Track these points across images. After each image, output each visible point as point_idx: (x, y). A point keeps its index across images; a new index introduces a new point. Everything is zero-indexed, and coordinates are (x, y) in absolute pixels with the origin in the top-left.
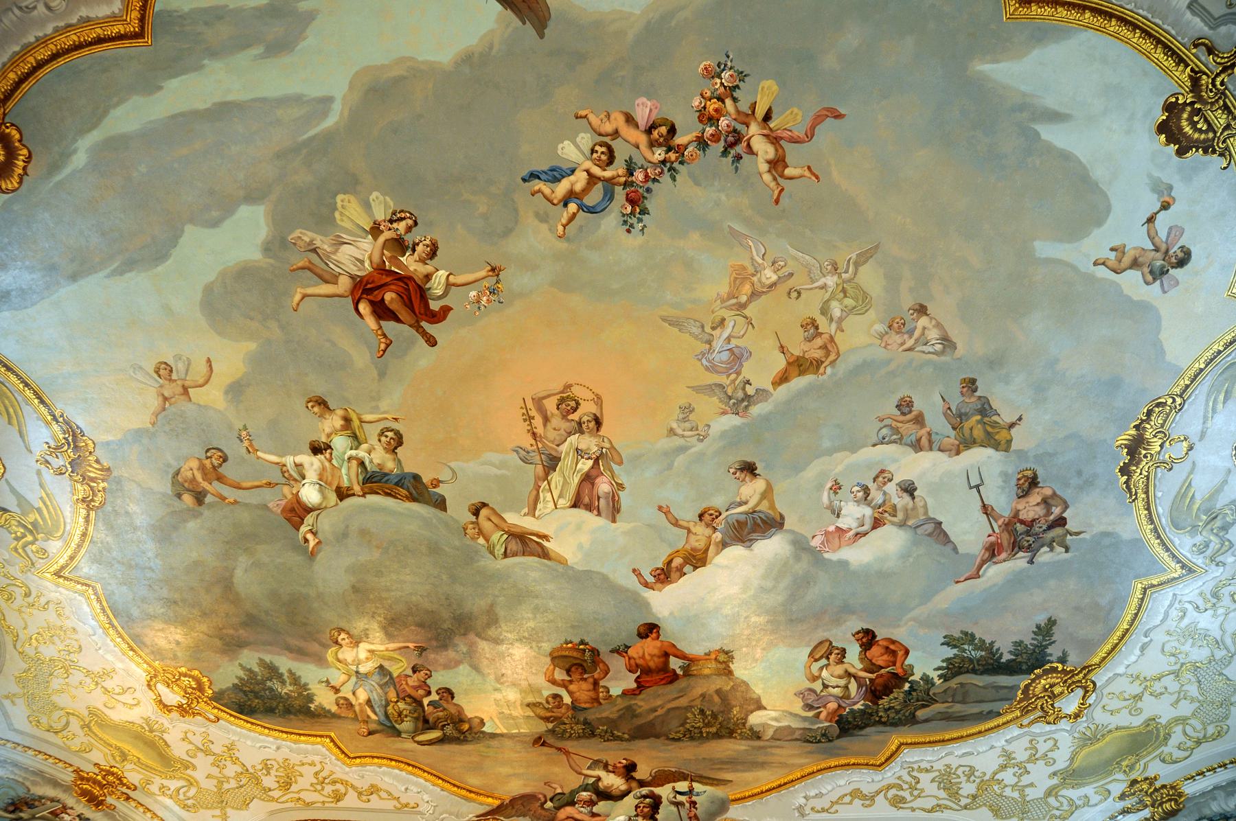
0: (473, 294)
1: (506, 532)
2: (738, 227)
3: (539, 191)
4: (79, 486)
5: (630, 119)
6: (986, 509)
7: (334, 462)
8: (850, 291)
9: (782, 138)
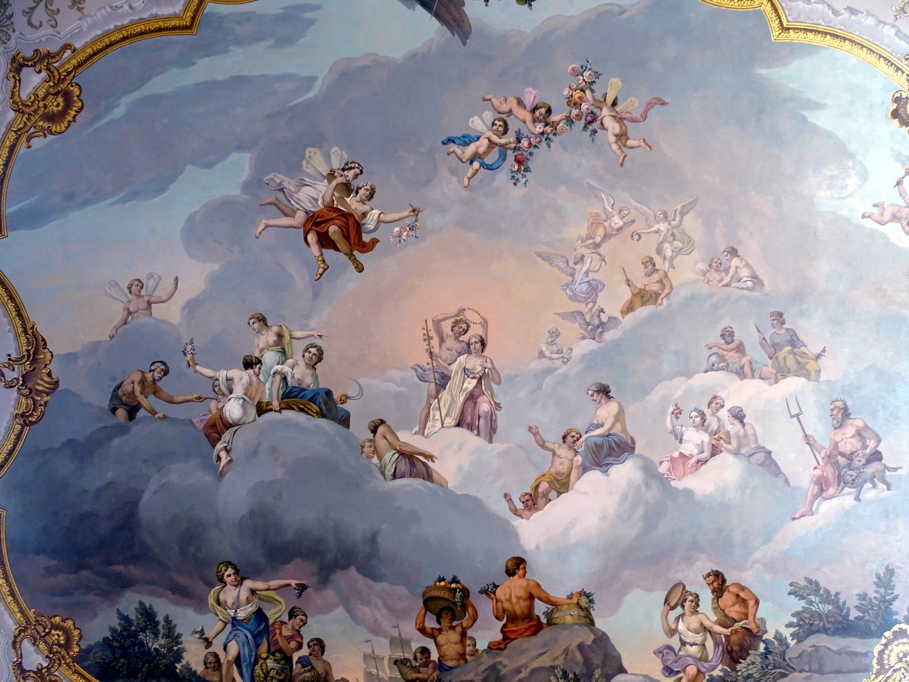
0: (397, 229)
1: (398, 452)
2: (594, 183)
3: (453, 152)
4: (23, 400)
5: (520, 103)
6: (808, 440)
7: (261, 377)
8: (678, 235)
9: (625, 119)
